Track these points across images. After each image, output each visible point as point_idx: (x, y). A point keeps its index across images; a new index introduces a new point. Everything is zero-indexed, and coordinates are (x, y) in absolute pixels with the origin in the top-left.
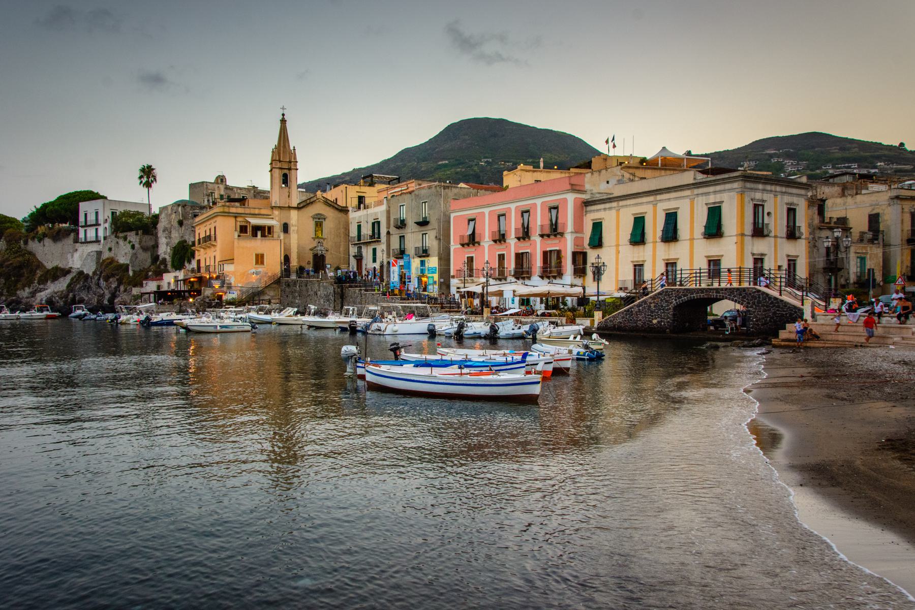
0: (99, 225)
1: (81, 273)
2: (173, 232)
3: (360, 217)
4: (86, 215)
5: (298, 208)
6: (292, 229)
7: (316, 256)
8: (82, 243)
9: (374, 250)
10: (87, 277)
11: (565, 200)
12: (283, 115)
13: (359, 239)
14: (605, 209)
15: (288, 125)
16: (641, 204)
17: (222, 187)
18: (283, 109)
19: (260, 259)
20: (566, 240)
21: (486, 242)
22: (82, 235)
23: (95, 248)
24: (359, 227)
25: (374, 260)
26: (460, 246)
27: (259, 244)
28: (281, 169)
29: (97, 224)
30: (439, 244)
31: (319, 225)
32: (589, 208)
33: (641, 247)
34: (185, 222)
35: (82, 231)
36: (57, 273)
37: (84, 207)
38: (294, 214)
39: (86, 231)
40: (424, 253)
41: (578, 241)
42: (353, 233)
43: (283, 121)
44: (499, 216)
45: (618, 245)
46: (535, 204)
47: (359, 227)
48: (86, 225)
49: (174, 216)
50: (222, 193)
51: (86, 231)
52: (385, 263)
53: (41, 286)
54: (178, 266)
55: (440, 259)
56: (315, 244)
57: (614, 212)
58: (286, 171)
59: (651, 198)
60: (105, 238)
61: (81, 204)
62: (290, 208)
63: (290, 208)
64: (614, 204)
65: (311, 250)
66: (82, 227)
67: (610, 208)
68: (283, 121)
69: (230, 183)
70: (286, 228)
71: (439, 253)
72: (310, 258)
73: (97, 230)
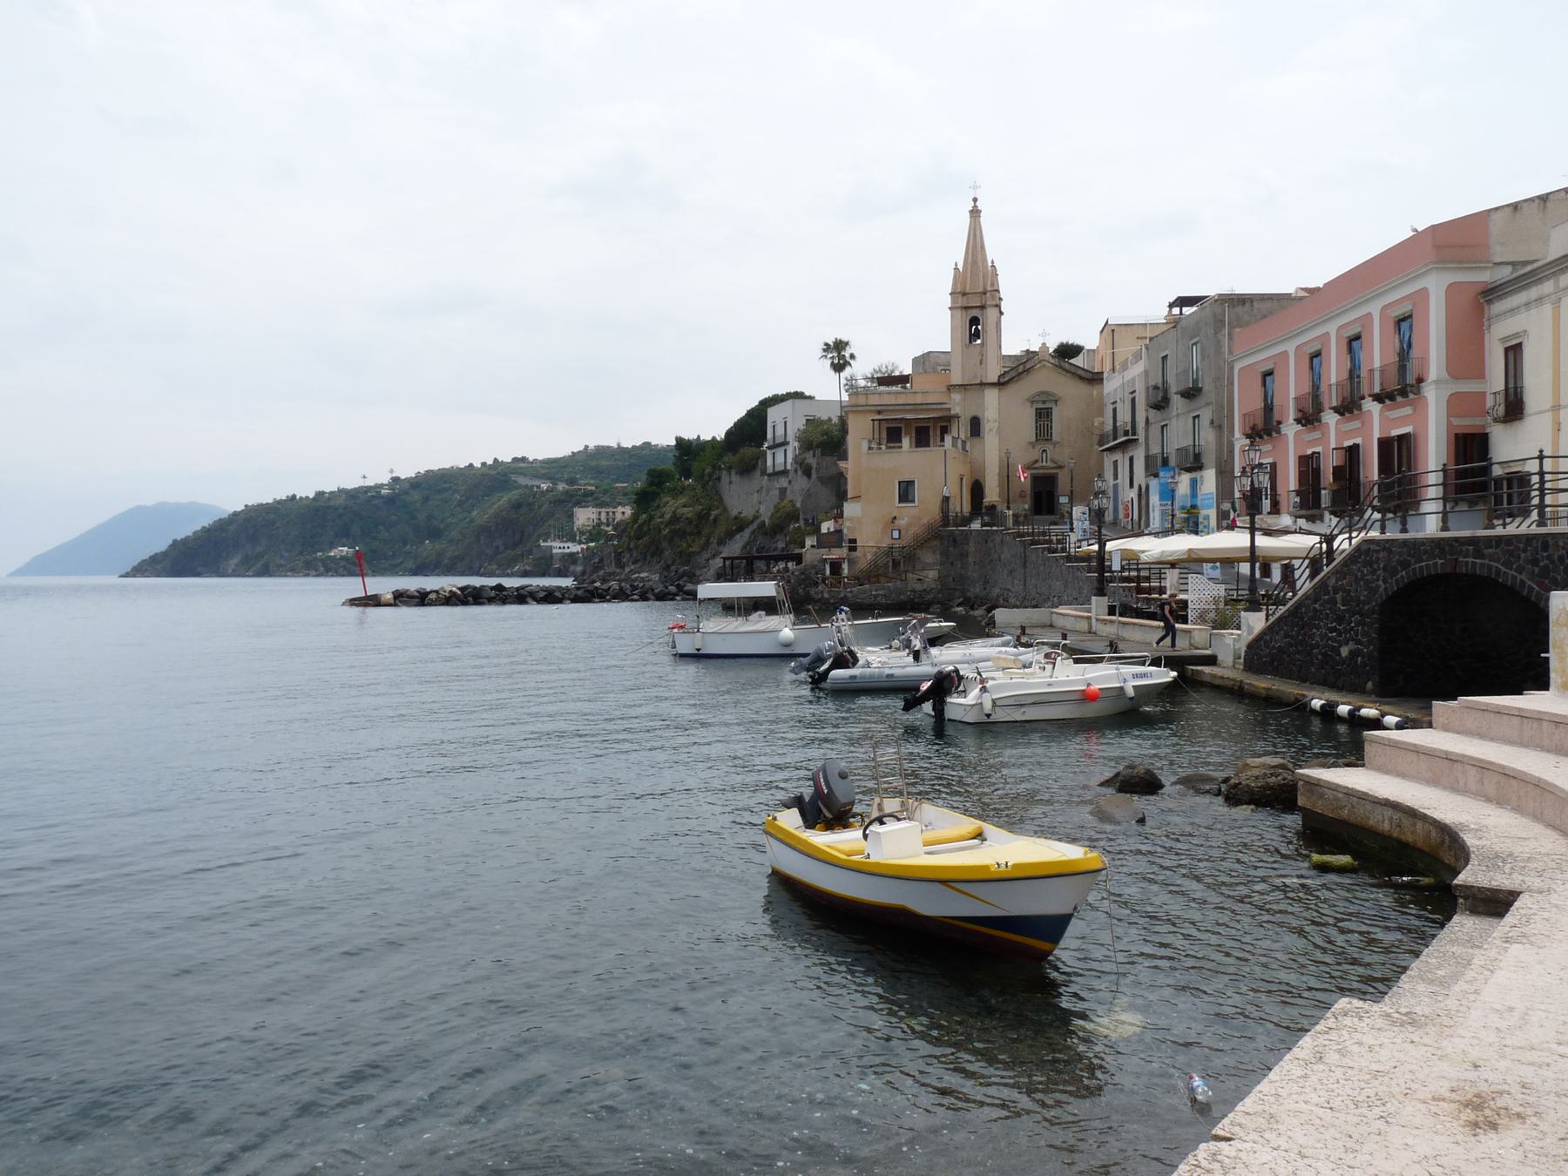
5: (1000, 384)
6: (989, 427)
7: (1036, 479)
11: (1424, 292)
12: (975, 200)
14: (1527, 304)
15: (983, 219)
18: (975, 187)
19: (906, 491)
24: (1115, 410)
25: (1131, 485)
28: (966, 308)
29: (785, 443)
32: (1499, 307)
37: (774, 415)
38: (991, 396)
41: (1455, 404)
43: (975, 213)
44: (1312, 359)
56: (1035, 454)
57: (1547, 309)
58: (975, 313)
63: (983, 385)
64: (1548, 287)
67: (1540, 300)
68: (975, 213)
70: (976, 426)
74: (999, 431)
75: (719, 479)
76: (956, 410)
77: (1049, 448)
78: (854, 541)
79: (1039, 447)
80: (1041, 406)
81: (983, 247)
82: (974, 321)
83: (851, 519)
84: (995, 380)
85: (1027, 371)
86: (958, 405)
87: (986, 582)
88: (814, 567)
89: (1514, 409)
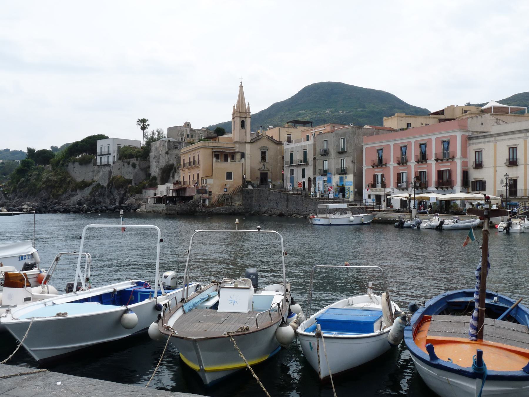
0: (110, 154)
1: (99, 185)
2: (161, 158)
3: (292, 148)
4: (101, 148)
5: (251, 143)
7: (262, 174)
9: (304, 171)
10: (102, 187)
11: (455, 137)
12: (241, 83)
13: (292, 161)
14: (484, 142)
16: (515, 138)
17: (188, 129)
18: (241, 79)
19: (229, 176)
20: (456, 163)
21: (392, 164)
22: (98, 160)
23: (108, 169)
24: (292, 155)
25: (304, 176)
26: (371, 167)
27: (229, 166)
28: (241, 117)
29: (109, 154)
30: (354, 166)
31: (264, 154)
32: (472, 142)
33: (514, 168)
34: (169, 152)
35: (98, 159)
36: (84, 185)
37: (100, 143)
38: (248, 146)
39: (101, 158)
40: (343, 172)
41: (464, 164)
42: (287, 158)
43: (241, 87)
45: (495, 167)
46: (431, 139)
47: (292, 155)
48: (101, 155)
49: (162, 148)
50: (188, 133)
51: (101, 158)
52: (312, 178)
53: (73, 193)
54: (164, 181)
55: (354, 176)
56: (261, 166)
57: (492, 144)
58: (243, 119)
59: (522, 135)
60: (114, 163)
61: (98, 141)
63: (246, 142)
64: (492, 139)
65: (259, 170)
66: (99, 155)
67: (489, 142)
68: (241, 87)
69: (193, 127)
70: (243, 155)
71: (354, 172)
72: (258, 174)
73: (108, 157)
74: (251, 158)
75: (67, 166)
76: (237, 150)
77: (265, 164)
78: (211, 192)
79: (263, 163)
83: (209, 184)
86: (237, 148)
87: (260, 206)
88: (197, 200)
89: (479, 165)
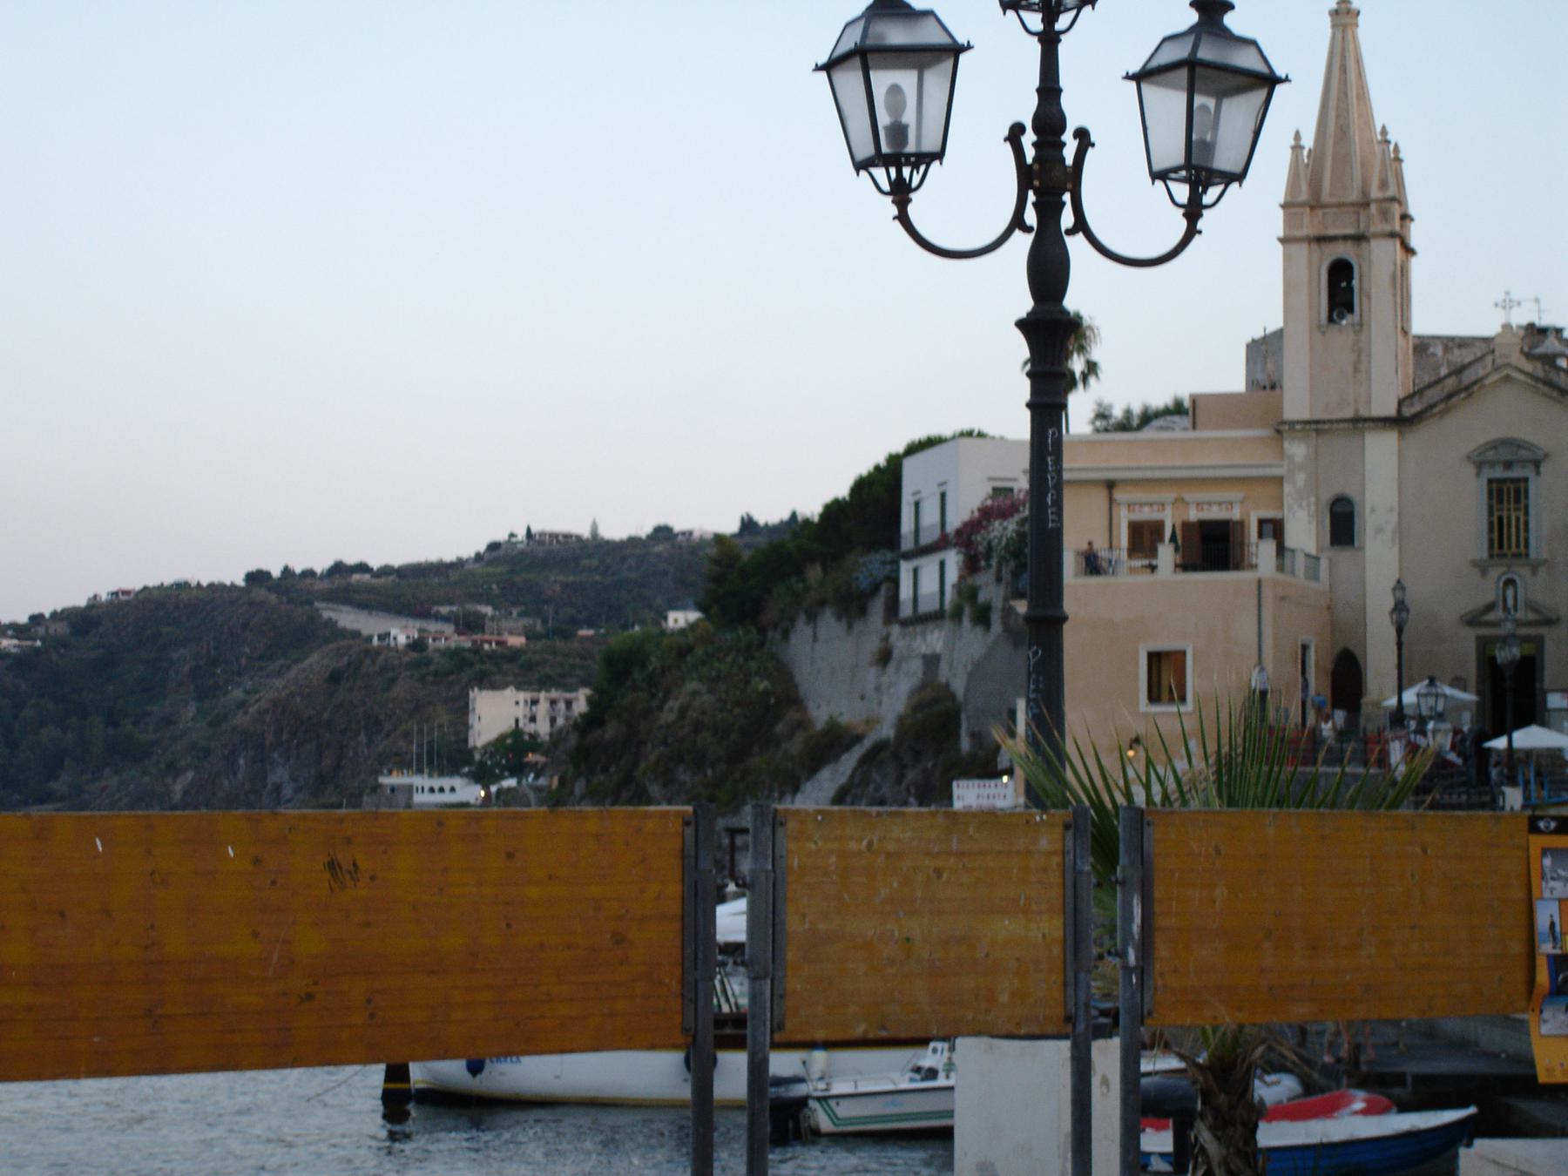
4: (917, 505)
5: (1400, 422)
8: (905, 623)
15: (1367, 33)
19: (1165, 675)
28: (1321, 240)
37: (914, 479)
38: (1381, 448)
56: (1486, 590)
62: (1360, 423)
63: (1360, 423)
65: (1473, 620)
70: (1342, 524)
74: (1402, 532)
77: (1521, 573)
80: (1499, 473)
81: (1363, 96)
82: (1340, 273)
84: (1390, 410)
85: (1468, 390)
